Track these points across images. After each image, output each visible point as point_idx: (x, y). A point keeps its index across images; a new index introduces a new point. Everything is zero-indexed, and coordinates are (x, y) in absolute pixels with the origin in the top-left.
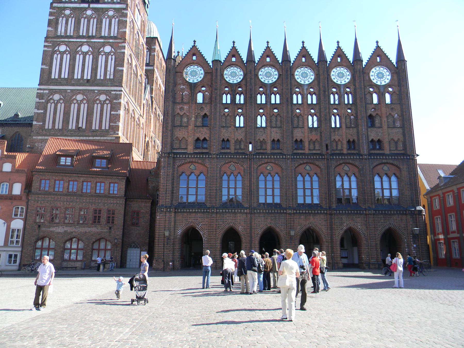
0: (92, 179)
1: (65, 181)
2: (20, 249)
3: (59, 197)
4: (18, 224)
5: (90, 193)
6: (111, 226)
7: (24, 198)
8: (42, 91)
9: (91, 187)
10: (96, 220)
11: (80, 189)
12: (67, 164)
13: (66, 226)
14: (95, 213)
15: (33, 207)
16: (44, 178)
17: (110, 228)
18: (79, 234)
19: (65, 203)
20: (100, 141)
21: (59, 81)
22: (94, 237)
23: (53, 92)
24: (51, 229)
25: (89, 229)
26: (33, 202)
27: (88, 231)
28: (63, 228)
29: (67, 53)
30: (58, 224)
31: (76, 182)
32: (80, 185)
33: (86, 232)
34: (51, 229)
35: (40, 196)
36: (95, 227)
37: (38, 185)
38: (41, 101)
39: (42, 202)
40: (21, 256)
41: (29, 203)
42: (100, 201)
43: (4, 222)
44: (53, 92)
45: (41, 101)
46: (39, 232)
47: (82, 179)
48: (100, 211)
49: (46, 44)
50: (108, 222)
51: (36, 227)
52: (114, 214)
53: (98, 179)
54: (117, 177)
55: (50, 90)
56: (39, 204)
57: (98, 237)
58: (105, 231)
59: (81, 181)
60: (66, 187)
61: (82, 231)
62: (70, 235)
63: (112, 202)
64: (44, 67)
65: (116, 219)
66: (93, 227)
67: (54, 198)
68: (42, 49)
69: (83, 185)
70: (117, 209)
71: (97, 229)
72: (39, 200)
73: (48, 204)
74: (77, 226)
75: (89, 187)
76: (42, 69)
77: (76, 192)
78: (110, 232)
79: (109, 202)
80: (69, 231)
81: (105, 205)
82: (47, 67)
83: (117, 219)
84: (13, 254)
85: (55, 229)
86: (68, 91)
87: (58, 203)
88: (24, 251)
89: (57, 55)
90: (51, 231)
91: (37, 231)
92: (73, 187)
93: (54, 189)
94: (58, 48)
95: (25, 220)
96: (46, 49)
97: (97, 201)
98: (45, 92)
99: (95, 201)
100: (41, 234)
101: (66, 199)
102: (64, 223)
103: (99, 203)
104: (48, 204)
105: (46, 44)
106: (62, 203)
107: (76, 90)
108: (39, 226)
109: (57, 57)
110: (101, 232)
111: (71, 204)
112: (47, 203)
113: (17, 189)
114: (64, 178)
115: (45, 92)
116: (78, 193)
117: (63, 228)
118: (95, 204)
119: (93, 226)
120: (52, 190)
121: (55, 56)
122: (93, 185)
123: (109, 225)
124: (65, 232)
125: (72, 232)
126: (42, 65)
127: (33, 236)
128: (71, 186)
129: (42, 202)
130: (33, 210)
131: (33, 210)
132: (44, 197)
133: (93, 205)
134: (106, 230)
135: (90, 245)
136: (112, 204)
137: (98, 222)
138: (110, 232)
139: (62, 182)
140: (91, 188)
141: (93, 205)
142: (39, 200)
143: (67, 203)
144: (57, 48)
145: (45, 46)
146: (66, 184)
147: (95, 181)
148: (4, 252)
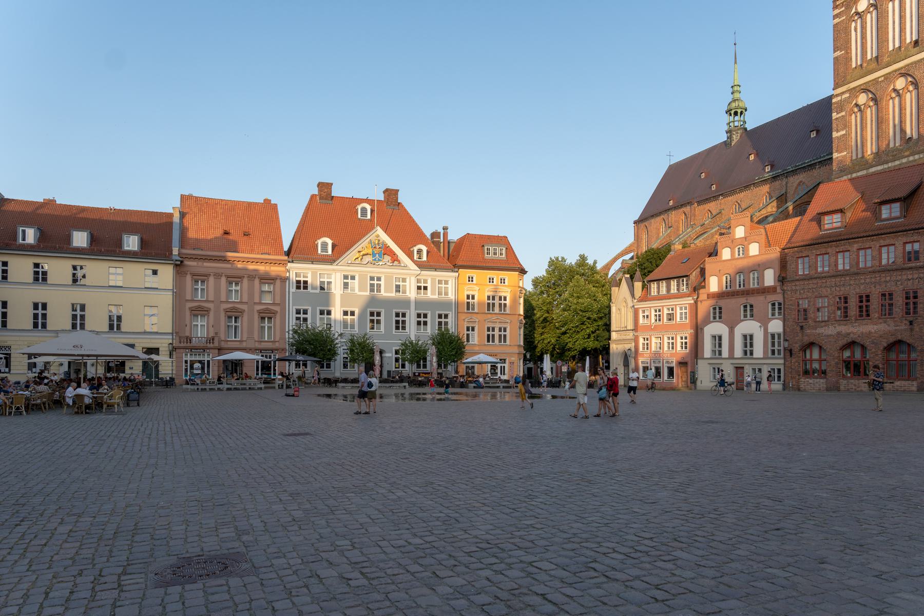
0: (872, 243)
1: (830, 254)
2: (782, 361)
3: (824, 281)
4: (776, 326)
5: (871, 267)
6: (911, 319)
7: (779, 290)
8: (839, 98)
9: (872, 257)
10: (887, 310)
11: (854, 264)
12: (835, 225)
13: (840, 325)
14: (861, 301)
15: (791, 300)
16: (800, 256)
17: (911, 323)
18: (859, 336)
19: (833, 289)
20: (902, 166)
21: (863, 70)
22: (885, 340)
23: (854, 92)
24: (819, 331)
25: (875, 327)
26: (789, 293)
27: (873, 331)
28: (835, 327)
29: (871, 9)
30: (827, 323)
31: (848, 253)
32: (854, 256)
33: (870, 333)
34: (819, 331)
35: (797, 283)
36: (885, 322)
37: (794, 266)
38: (840, 115)
39: (802, 292)
40: (785, 370)
41: (786, 296)
42: (888, 278)
43: (760, 324)
44: (854, 92)
45: (840, 115)
46: (803, 336)
47: (856, 246)
48: (891, 295)
49: (837, 11)
50: (908, 313)
51: (798, 328)
52: (915, 297)
53: (882, 242)
54: (916, 231)
55: (850, 91)
56: (798, 295)
57: (892, 340)
58: (902, 328)
59: (855, 249)
60: (833, 264)
61: (864, 331)
62: (846, 339)
63: (910, 277)
64: (838, 53)
65: (920, 306)
66: (881, 323)
67: (817, 283)
68: (832, 22)
69: (858, 256)
70: (921, 288)
71: (889, 325)
72: (797, 290)
73: (810, 294)
74: (855, 323)
75: (869, 258)
76: (836, 60)
77: (849, 270)
78: (912, 330)
79: (905, 277)
80: (843, 332)
81: (899, 283)
82: (843, 52)
83: (921, 305)
84: (776, 367)
85: (823, 331)
86: (880, 80)
87: (824, 290)
88: (787, 363)
89: (855, 21)
90: (819, 334)
91: (800, 335)
92: (843, 263)
93: (817, 269)
94: (856, 9)
95: (784, 321)
96: (837, 20)
97: (883, 279)
98: (844, 96)
99: (880, 279)
100: (806, 340)
101: (834, 283)
102: (836, 321)
103: (886, 282)
104: (810, 294)
105: (837, 11)
106: (829, 290)
107: (893, 72)
108: (802, 327)
109: (855, 27)
110: (896, 330)
111: (843, 289)
112: (808, 292)
113: (770, 278)
114: (829, 250)
115: (844, 96)
116: (852, 270)
117: (835, 327)
118: (880, 285)
119: (881, 321)
120: (813, 272)
121: (853, 24)
122: (876, 253)
123: (908, 318)
124: (839, 334)
125: (849, 334)
126: (835, 51)
127: (796, 343)
128: (840, 261)
129: (802, 292)
130: (791, 305)
131: (791, 305)
132: (804, 284)
133: (878, 287)
134: (904, 326)
135: (880, 352)
136: (910, 280)
137: (889, 314)
138: (912, 330)
139: (826, 257)
140: (873, 258)
141: (878, 287)
142: (797, 290)
143: (837, 288)
144: (854, 11)
145: (835, 17)
146: (833, 259)
147: (878, 246)
148: (765, 366)
